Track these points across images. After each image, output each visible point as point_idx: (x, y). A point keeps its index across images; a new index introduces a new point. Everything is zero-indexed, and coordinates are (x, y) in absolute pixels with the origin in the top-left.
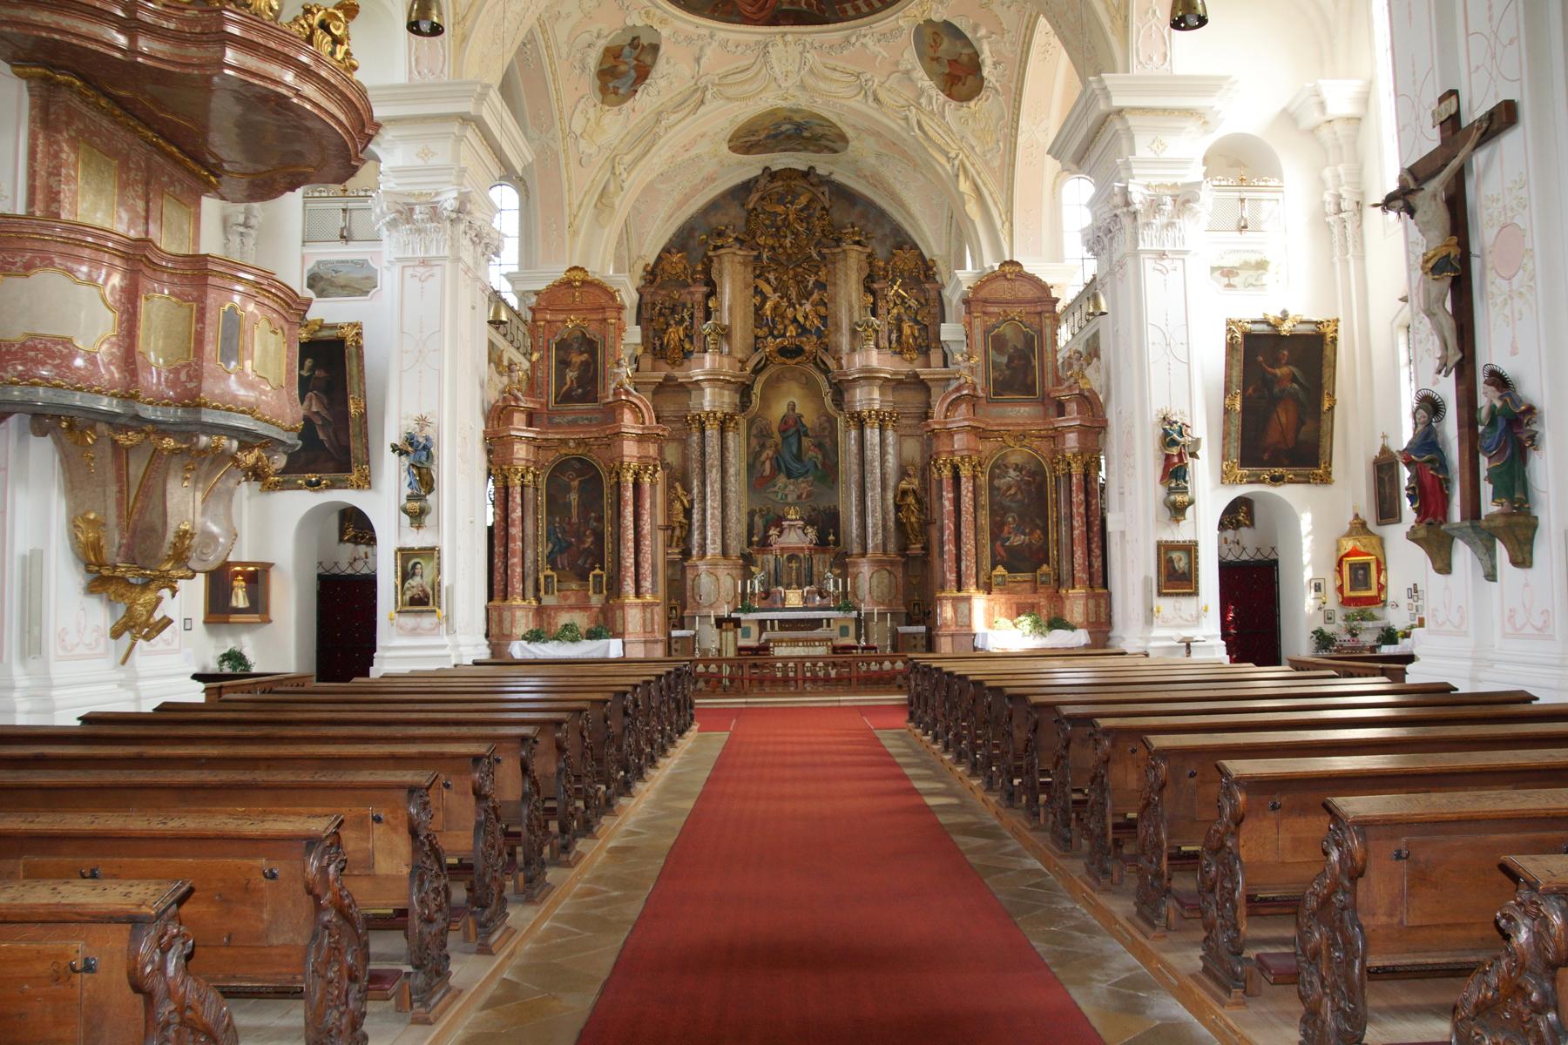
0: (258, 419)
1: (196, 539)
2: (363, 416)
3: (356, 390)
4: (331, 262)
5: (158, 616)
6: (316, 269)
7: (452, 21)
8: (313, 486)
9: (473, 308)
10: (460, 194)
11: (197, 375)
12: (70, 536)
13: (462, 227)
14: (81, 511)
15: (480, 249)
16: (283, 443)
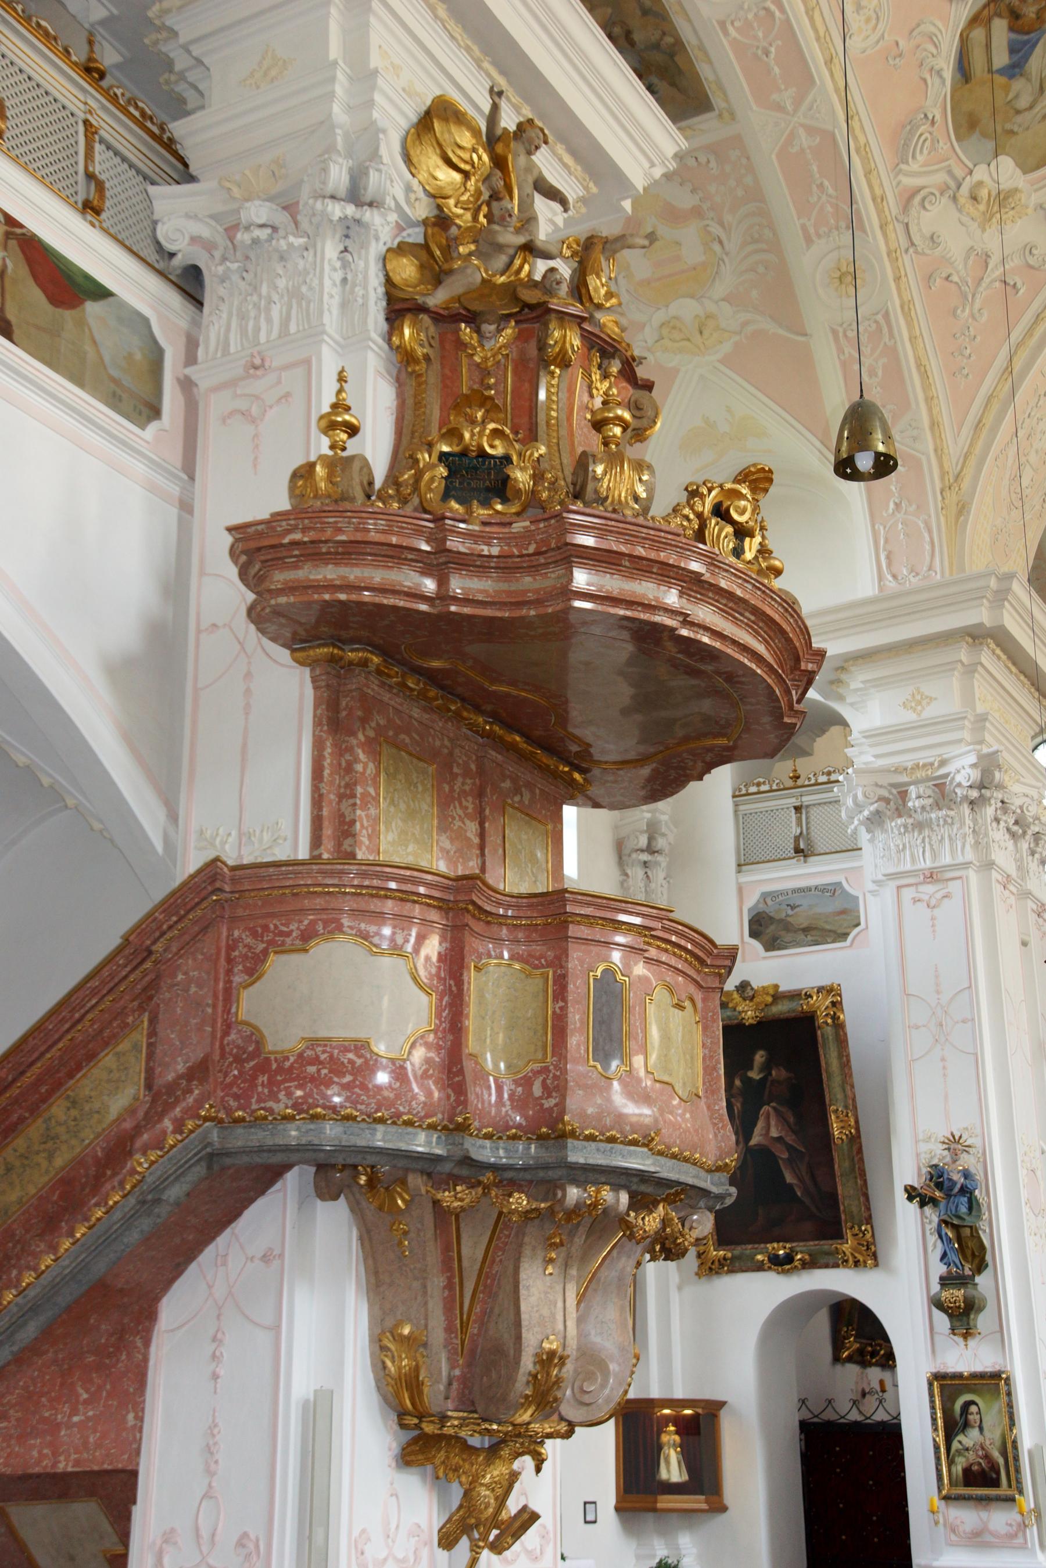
0: (660, 1153)
1: (569, 1367)
2: (855, 1139)
3: (840, 1096)
4: (781, 893)
5: (513, 1505)
6: (762, 907)
7: (938, 486)
8: (782, 1264)
9: (1024, 944)
10: (981, 757)
11: (557, 1086)
12: (373, 1365)
13: (990, 811)
14: (389, 1323)
15: (1024, 845)
16: (705, 1193)
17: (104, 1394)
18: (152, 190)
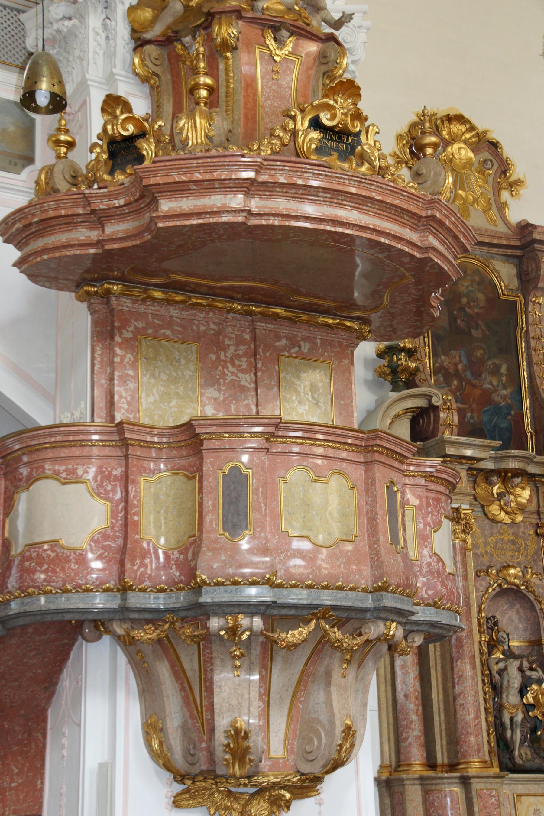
17: (26, 769)
18: (22, 17)
